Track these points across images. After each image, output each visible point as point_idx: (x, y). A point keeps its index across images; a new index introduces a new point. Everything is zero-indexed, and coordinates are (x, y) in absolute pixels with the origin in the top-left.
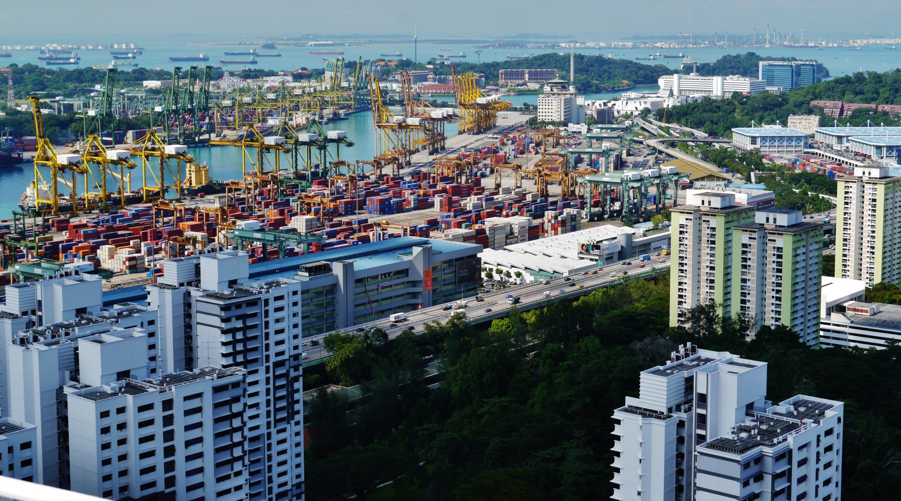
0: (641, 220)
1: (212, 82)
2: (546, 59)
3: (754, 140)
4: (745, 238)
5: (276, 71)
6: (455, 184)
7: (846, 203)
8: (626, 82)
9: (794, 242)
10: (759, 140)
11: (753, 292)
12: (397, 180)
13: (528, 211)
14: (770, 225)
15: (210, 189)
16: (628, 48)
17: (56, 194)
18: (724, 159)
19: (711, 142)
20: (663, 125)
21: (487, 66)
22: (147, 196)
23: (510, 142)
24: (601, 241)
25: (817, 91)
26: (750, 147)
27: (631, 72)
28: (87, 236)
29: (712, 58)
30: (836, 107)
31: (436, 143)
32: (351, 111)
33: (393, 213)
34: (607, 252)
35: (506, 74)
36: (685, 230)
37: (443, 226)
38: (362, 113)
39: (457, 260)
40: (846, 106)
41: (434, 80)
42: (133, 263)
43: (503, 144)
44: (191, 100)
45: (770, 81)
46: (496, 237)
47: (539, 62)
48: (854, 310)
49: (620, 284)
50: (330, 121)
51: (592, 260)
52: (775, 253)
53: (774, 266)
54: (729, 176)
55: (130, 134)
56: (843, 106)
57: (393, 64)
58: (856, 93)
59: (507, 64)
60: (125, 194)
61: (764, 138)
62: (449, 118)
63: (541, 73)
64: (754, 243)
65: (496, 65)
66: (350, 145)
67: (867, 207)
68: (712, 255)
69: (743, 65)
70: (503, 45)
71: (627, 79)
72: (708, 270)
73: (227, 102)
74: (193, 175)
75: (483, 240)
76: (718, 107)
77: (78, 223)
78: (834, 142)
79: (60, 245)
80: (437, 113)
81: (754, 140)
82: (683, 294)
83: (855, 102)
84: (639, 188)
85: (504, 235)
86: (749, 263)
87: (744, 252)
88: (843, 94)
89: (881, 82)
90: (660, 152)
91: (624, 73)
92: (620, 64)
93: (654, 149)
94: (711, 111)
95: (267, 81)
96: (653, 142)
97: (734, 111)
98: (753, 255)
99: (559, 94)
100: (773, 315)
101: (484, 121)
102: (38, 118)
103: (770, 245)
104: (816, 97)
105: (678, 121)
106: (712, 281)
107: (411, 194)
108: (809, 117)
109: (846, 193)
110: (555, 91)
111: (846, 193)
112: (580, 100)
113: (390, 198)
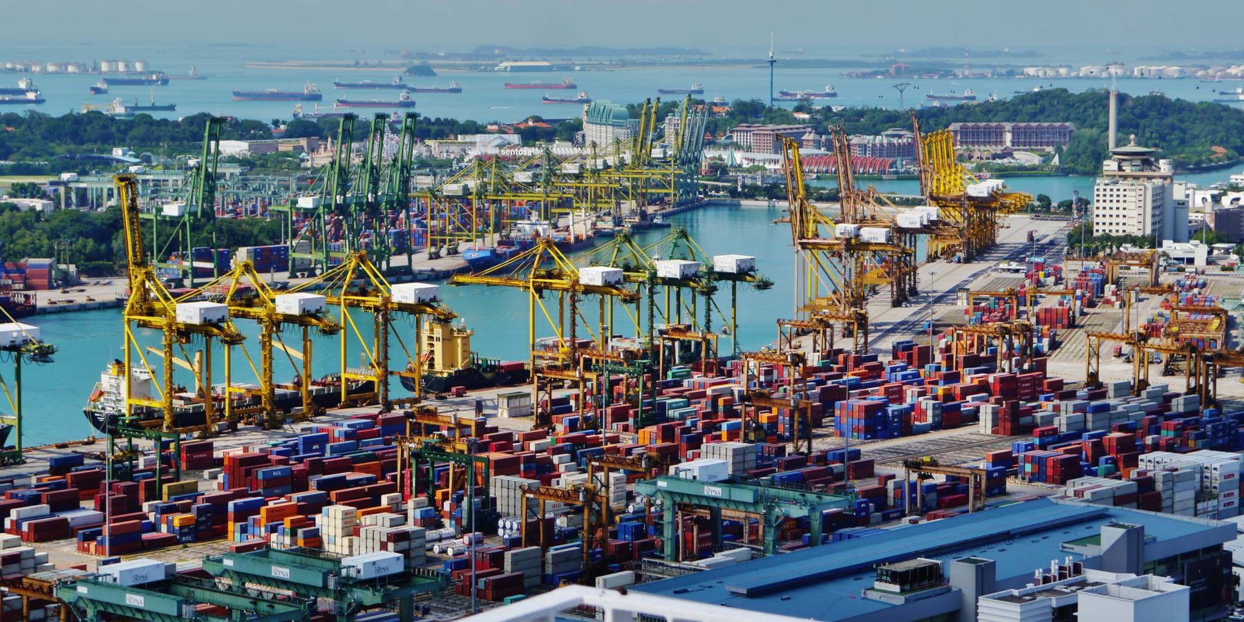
1: (355, 145)
2: (1045, 102)
5: (480, 123)
6: (998, 374)
8: (1220, 150)
13: (1198, 437)
16: (1170, 78)
17: (171, 389)
22: (349, 392)
23: (1052, 280)
27: (1228, 129)
28: (276, 486)
32: (669, 209)
33: (893, 437)
35: (964, 132)
37: (1028, 468)
38: (689, 215)
39: (1185, 556)
41: (818, 145)
42: (404, 545)
43: (1039, 284)
44: (375, 182)
46: (1178, 497)
47: (1030, 108)
57: (722, 111)
63: (1039, 132)
66: (764, 285)
70: (903, 71)
71: (1221, 143)
74: (438, 347)
77: (239, 452)
79: (231, 505)
85: (1192, 494)
91: (1214, 132)
92: (1204, 111)
95: (473, 144)
99: (1136, 178)
102: (132, 223)
107: (921, 394)
110: (1128, 169)
113: (885, 405)
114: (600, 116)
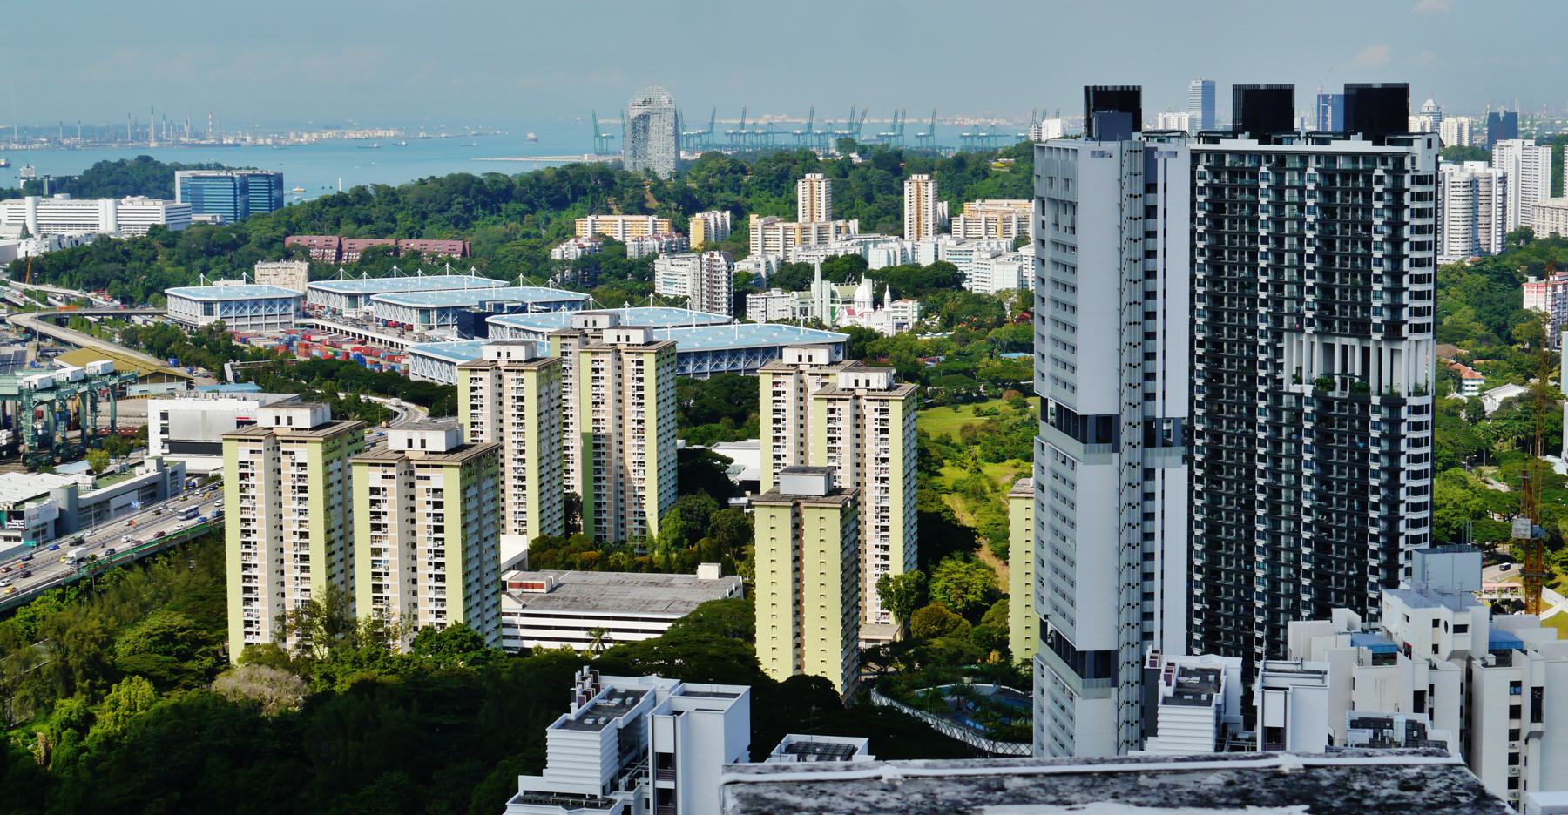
0: (58, 460)
3: (208, 308)
4: (374, 477)
7: (474, 407)
9: (462, 479)
10: (217, 307)
11: (394, 571)
14: (416, 453)
18: (169, 343)
19: (129, 316)
24: (22, 502)
25: (293, 219)
26: (204, 321)
29: (76, 168)
30: (329, 247)
34: (35, 522)
36: (249, 471)
40: (346, 244)
45: (198, 204)
48: (521, 585)
49: (84, 578)
51: (7, 539)
52: (431, 499)
53: (430, 521)
54: (182, 371)
56: (340, 245)
58: (360, 222)
61: (226, 304)
64: (391, 485)
67: (509, 410)
68: (303, 512)
69: (144, 178)
72: (296, 539)
76: (126, 253)
78: (343, 305)
81: (208, 308)
82: (253, 585)
83: (359, 236)
84: (51, 403)
86: (384, 520)
87: (373, 503)
88: (338, 223)
89: (397, 201)
90: (43, 337)
93: (28, 330)
94: (114, 259)
96: (25, 319)
97: (154, 259)
98: (391, 506)
100: (432, 606)
103: (420, 486)
104: (294, 229)
105: (56, 280)
106: (305, 558)
108: (290, 264)
109: (473, 389)
111: (473, 389)
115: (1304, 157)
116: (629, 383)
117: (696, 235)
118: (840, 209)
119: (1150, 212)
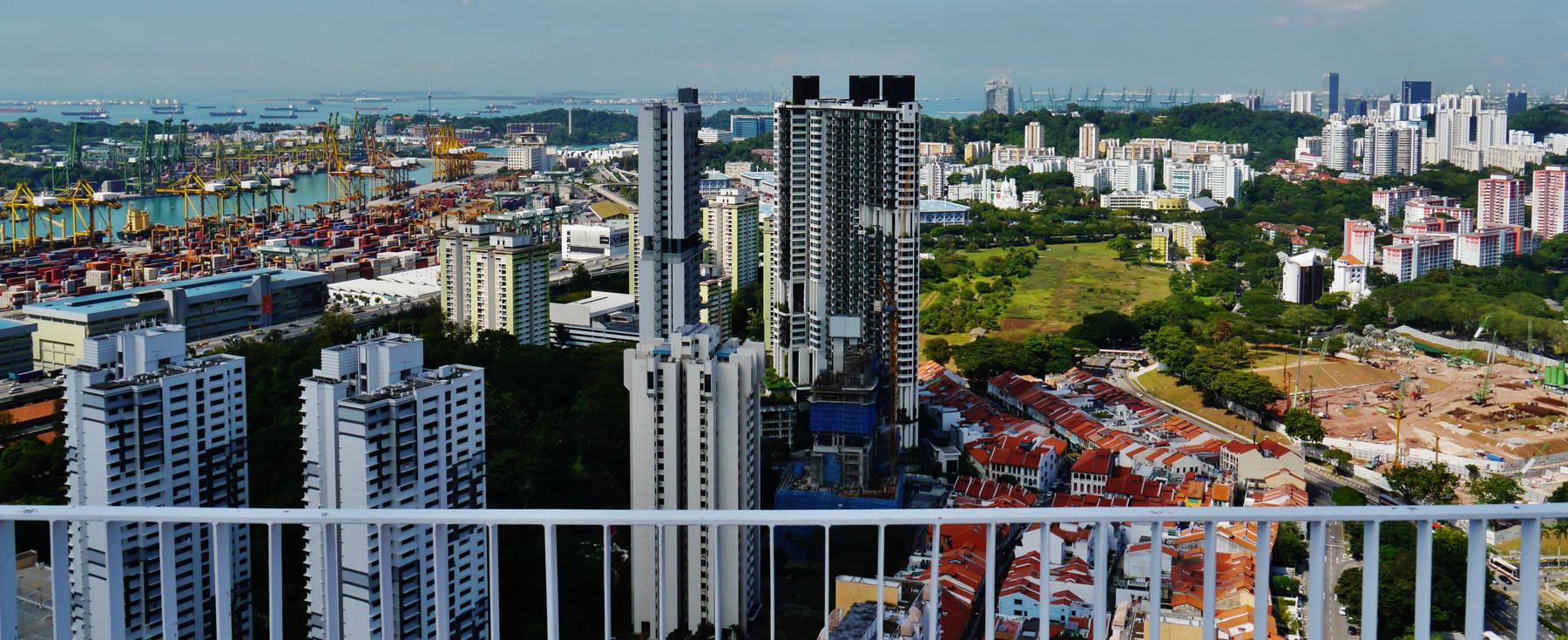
12: (331, 224)
15: (144, 235)
20: (620, 171)
21: (497, 120)
31: (399, 189)
45: (739, 132)
50: (323, 170)
55: (105, 184)
59: (518, 118)
60: (56, 239)
62: (409, 167)
65: (507, 119)
70: (541, 101)
73: (208, 154)
75: (367, 272)
78: (752, 184)
80: (396, 162)
101: (459, 169)
112: (551, 151)
114: (345, 121)
115: (865, 112)
116: (726, 224)
117: (968, 153)
118: (1046, 143)
119: (664, 137)
